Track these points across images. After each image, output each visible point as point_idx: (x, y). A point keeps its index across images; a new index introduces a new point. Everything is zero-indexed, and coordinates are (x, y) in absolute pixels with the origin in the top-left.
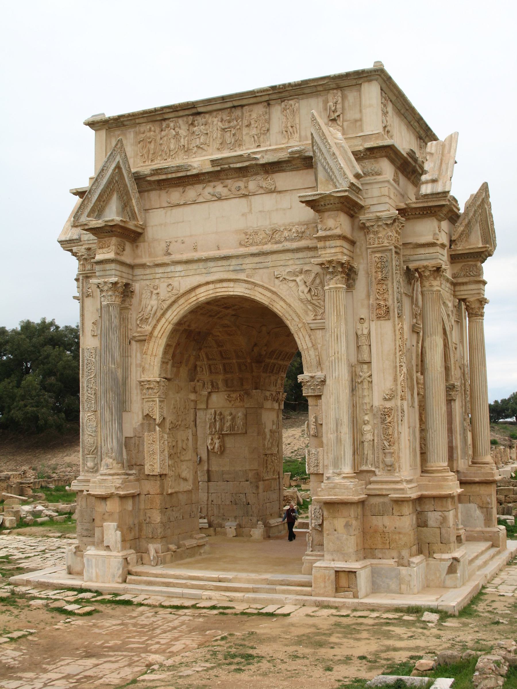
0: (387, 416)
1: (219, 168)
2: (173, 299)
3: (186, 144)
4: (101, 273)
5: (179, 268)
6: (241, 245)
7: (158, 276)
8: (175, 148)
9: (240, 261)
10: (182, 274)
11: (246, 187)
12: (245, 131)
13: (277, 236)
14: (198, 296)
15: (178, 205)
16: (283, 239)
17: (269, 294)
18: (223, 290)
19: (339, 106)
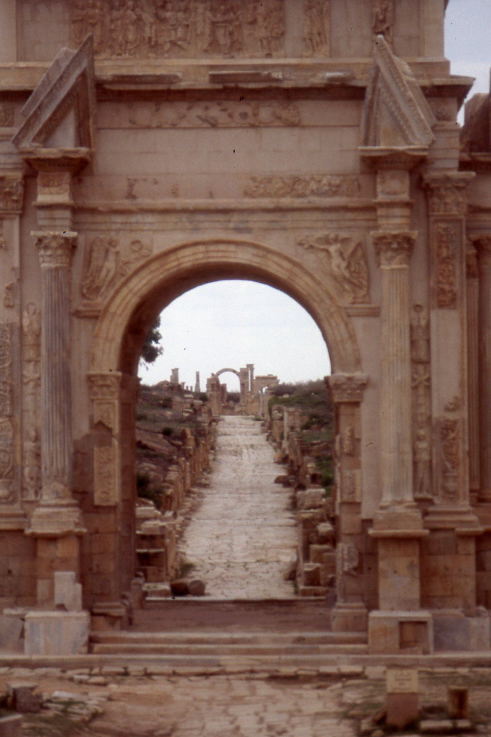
0: (450, 431)
1: (220, 86)
2: (142, 262)
3: (153, 35)
4: (46, 223)
5: (150, 218)
6: (246, 194)
7: (115, 227)
8: (136, 40)
9: (245, 217)
10: (155, 227)
11: (255, 115)
12: (246, 30)
13: (299, 188)
14: (182, 261)
15: (149, 128)
16: (308, 192)
17: (287, 265)
18: (219, 254)
19: (389, 15)
